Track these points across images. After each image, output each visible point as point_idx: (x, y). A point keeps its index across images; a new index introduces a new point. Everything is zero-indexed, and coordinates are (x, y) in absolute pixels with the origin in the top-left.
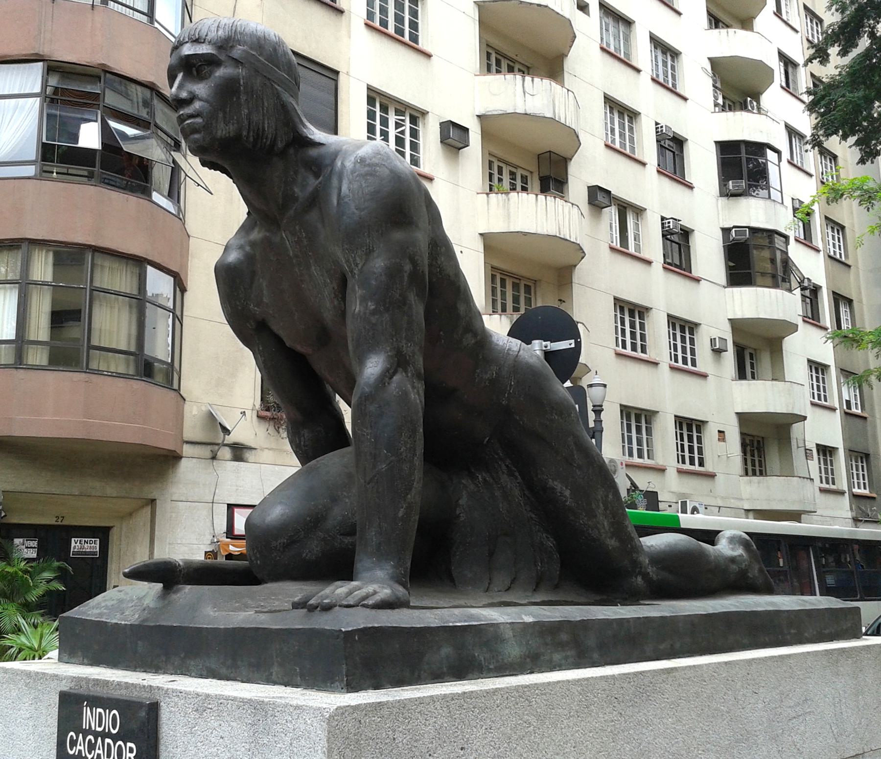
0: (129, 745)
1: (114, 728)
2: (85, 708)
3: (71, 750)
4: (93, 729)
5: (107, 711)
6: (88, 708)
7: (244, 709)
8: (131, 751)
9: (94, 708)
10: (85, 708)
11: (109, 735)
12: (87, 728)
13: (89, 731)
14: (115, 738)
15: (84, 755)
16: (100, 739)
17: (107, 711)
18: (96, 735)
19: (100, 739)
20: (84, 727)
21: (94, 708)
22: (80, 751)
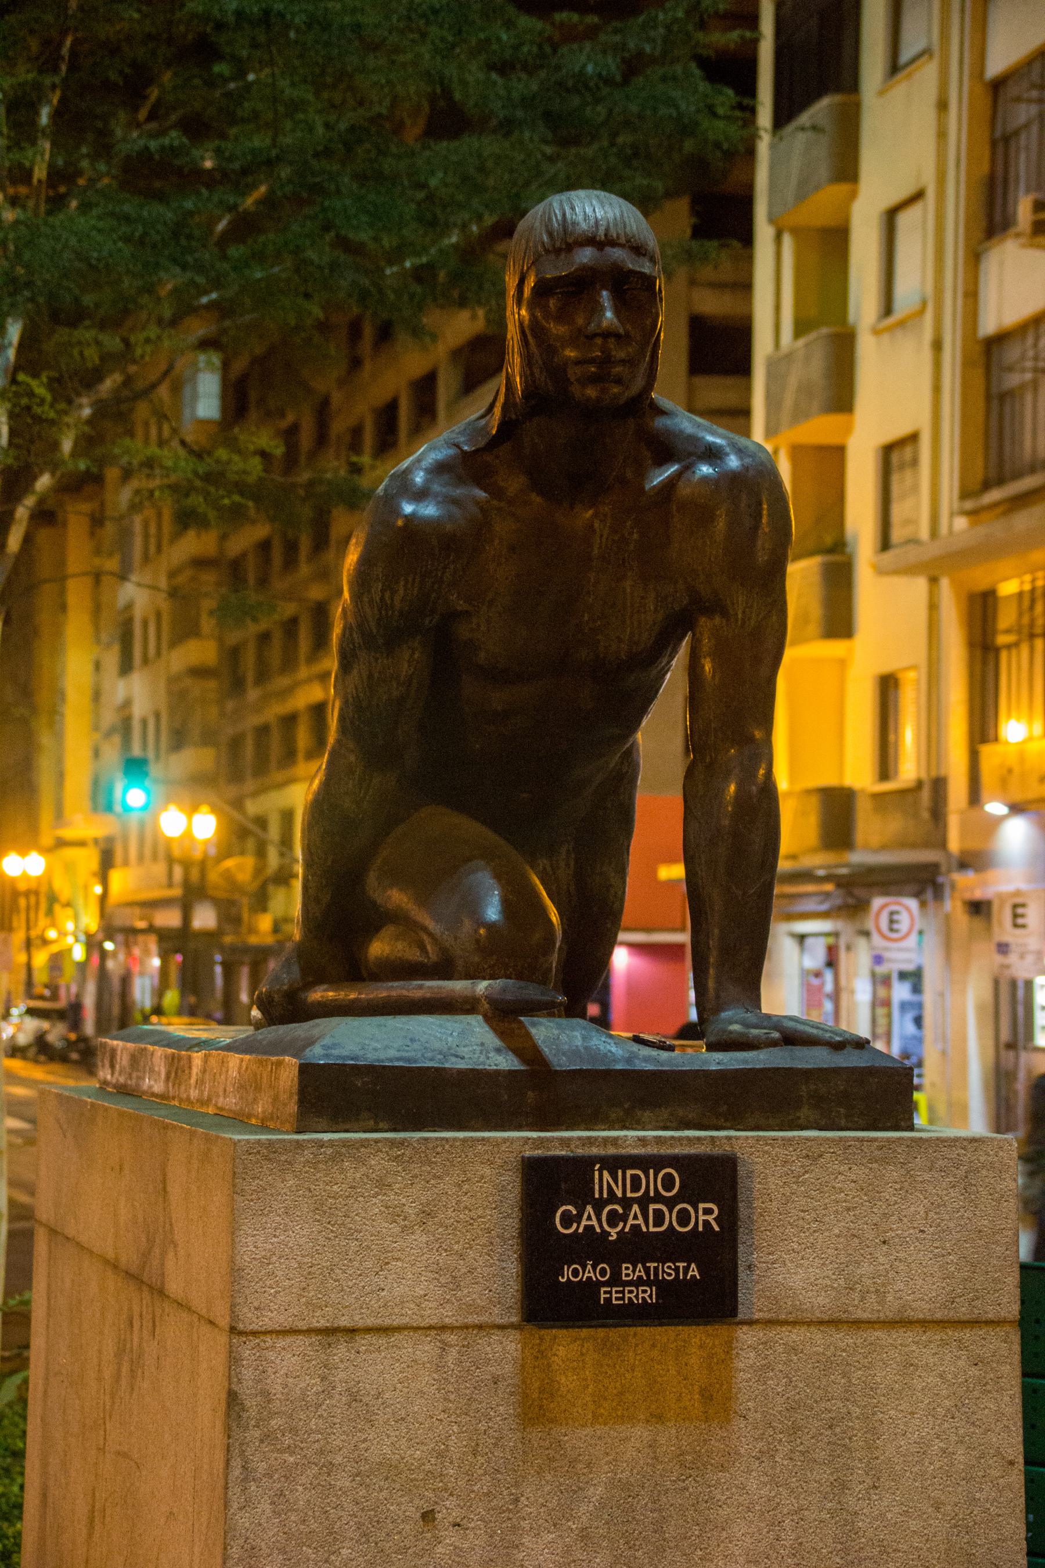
0: (701, 1206)
1: (668, 1190)
2: (597, 1173)
3: (567, 1226)
4: (619, 1194)
5: (651, 1171)
6: (606, 1174)
7: (890, 1149)
8: (708, 1212)
9: (620, 1173)
10: (597, 1173)
11: (658, 1198)
12: (605, 1196)
13: (612, 1198)
14: (670, 1203)
15: (598, 1230)
16: (635, 1208)
17: (651, 1171)
18: (626, 1203)
19: (635, 1208)
20: (597, 1196)
21: (620, 1173)
22: (589, 1229)
